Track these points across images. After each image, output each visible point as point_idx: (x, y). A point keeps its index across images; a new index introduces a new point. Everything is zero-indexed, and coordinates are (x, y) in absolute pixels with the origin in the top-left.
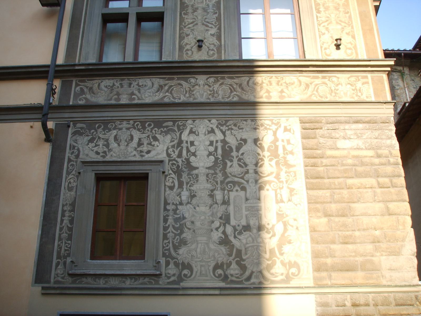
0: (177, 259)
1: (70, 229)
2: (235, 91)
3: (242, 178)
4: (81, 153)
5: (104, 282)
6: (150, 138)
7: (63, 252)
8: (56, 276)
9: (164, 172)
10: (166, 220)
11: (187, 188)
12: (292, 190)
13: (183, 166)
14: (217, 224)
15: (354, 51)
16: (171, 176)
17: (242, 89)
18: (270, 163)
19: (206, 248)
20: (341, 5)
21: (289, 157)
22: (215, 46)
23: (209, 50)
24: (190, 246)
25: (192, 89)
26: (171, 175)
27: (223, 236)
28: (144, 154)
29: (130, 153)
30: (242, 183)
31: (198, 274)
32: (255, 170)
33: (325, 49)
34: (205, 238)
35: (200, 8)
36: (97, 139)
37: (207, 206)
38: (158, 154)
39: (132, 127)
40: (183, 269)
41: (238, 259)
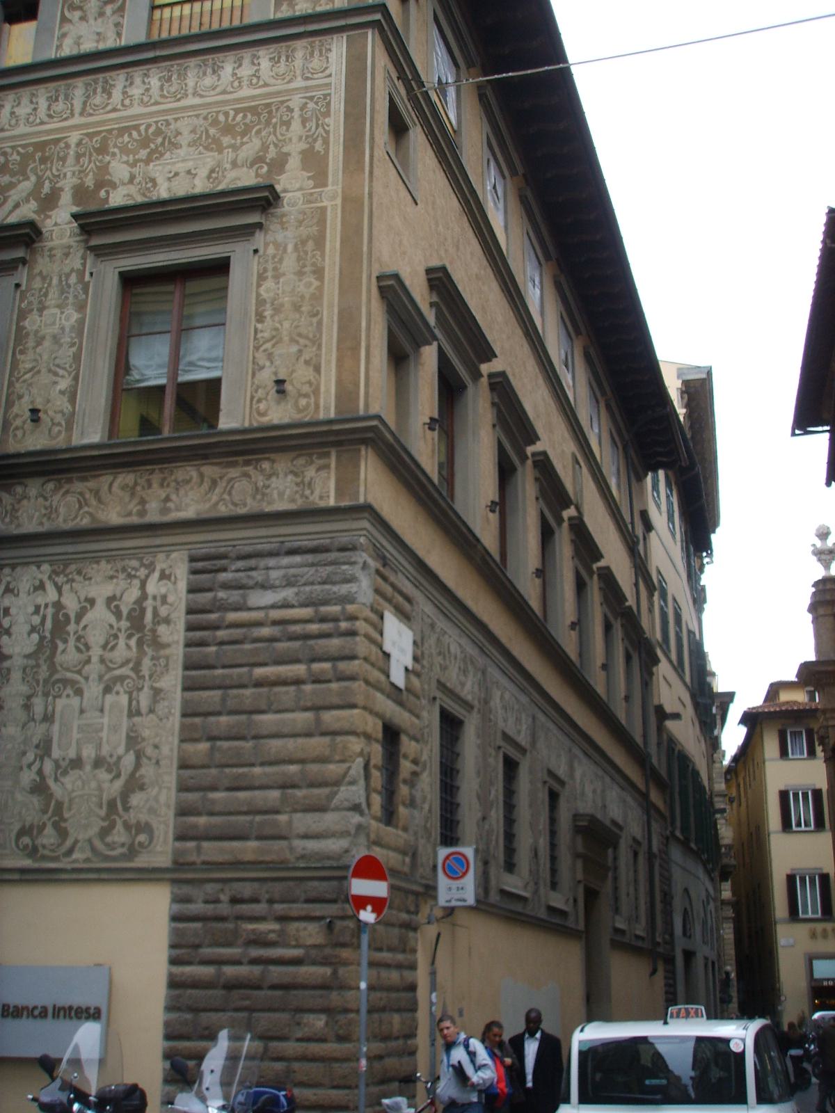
2: (86, 504)
3: (79, 672)
12: (157, 692)
14: (30, 756)
15: (313, 400)
17: (100, 501)
19: (10, 801)
20: (307, 296)
21: (162, 629)
22: (64, 414)
23: (53, 424)
25: (17, 506)
27: (38, 779)
32: (101, 656)
33: (259, 401)
35: (47, 337)
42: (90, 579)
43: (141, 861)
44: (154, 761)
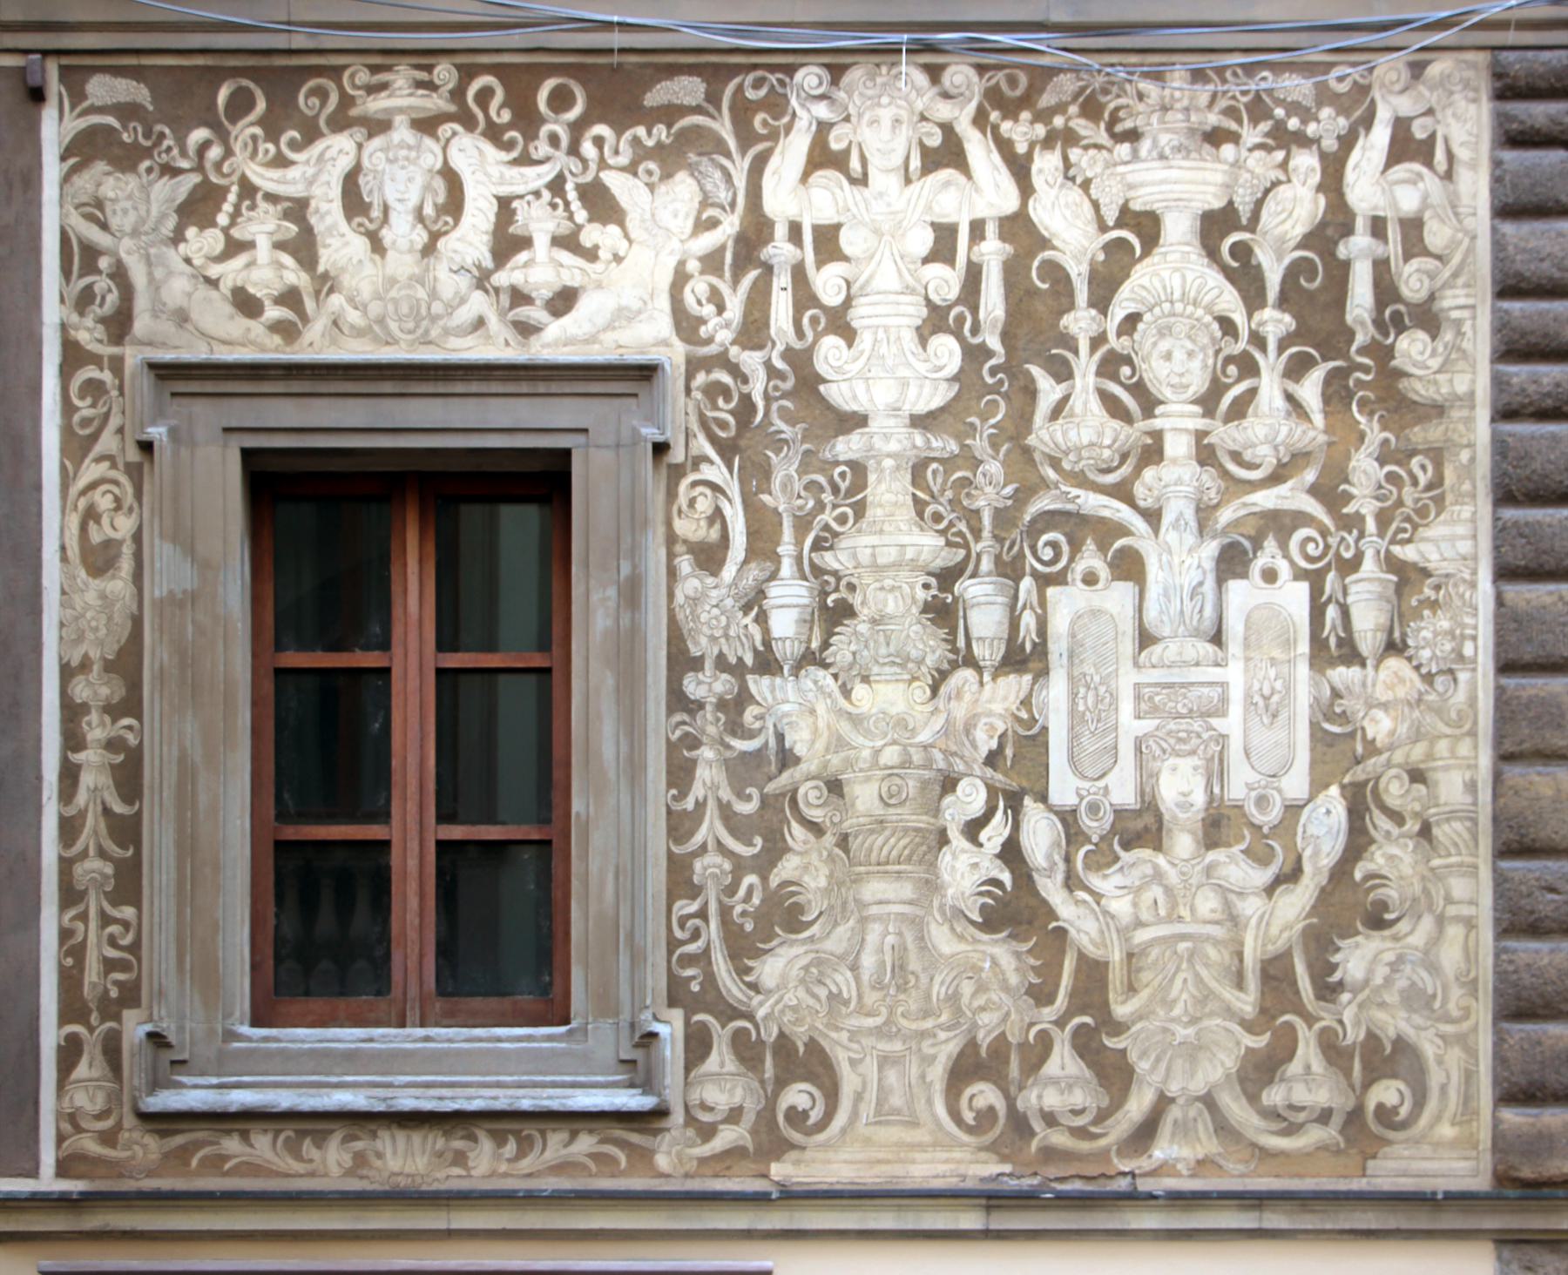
0: (750, 1017)
1: (127, 831)
3: (1122, 492)
4: (141, 303)
5: (347, 1159)
6: (572, 195)
7: (95, 979)
8: (67, 1127)
9: (660, 449)
10: (680, 773)
11: (799, 559)
12: (1406, 576)
13: (775, 406)
14: (971, 797)
16: (709, 473)
18: (1292, 387)
21: (1412, 347)
24: (821, 939)
26: (704, 467)
27: (1006, 877)
28: (535, 313)
29: (451, 309)
30: (1123, 530)
31: (867, 1110)
32: (1200, 435)
34: (907, 890)
36: (232, 197)
37: (915, 679)
38: (624, 316)
39: (452, 108)
40: (781, 1083)
41: (1087, 1019)
42: (1133, 136)
43: (1395, 1168)
44: (1412, 826)
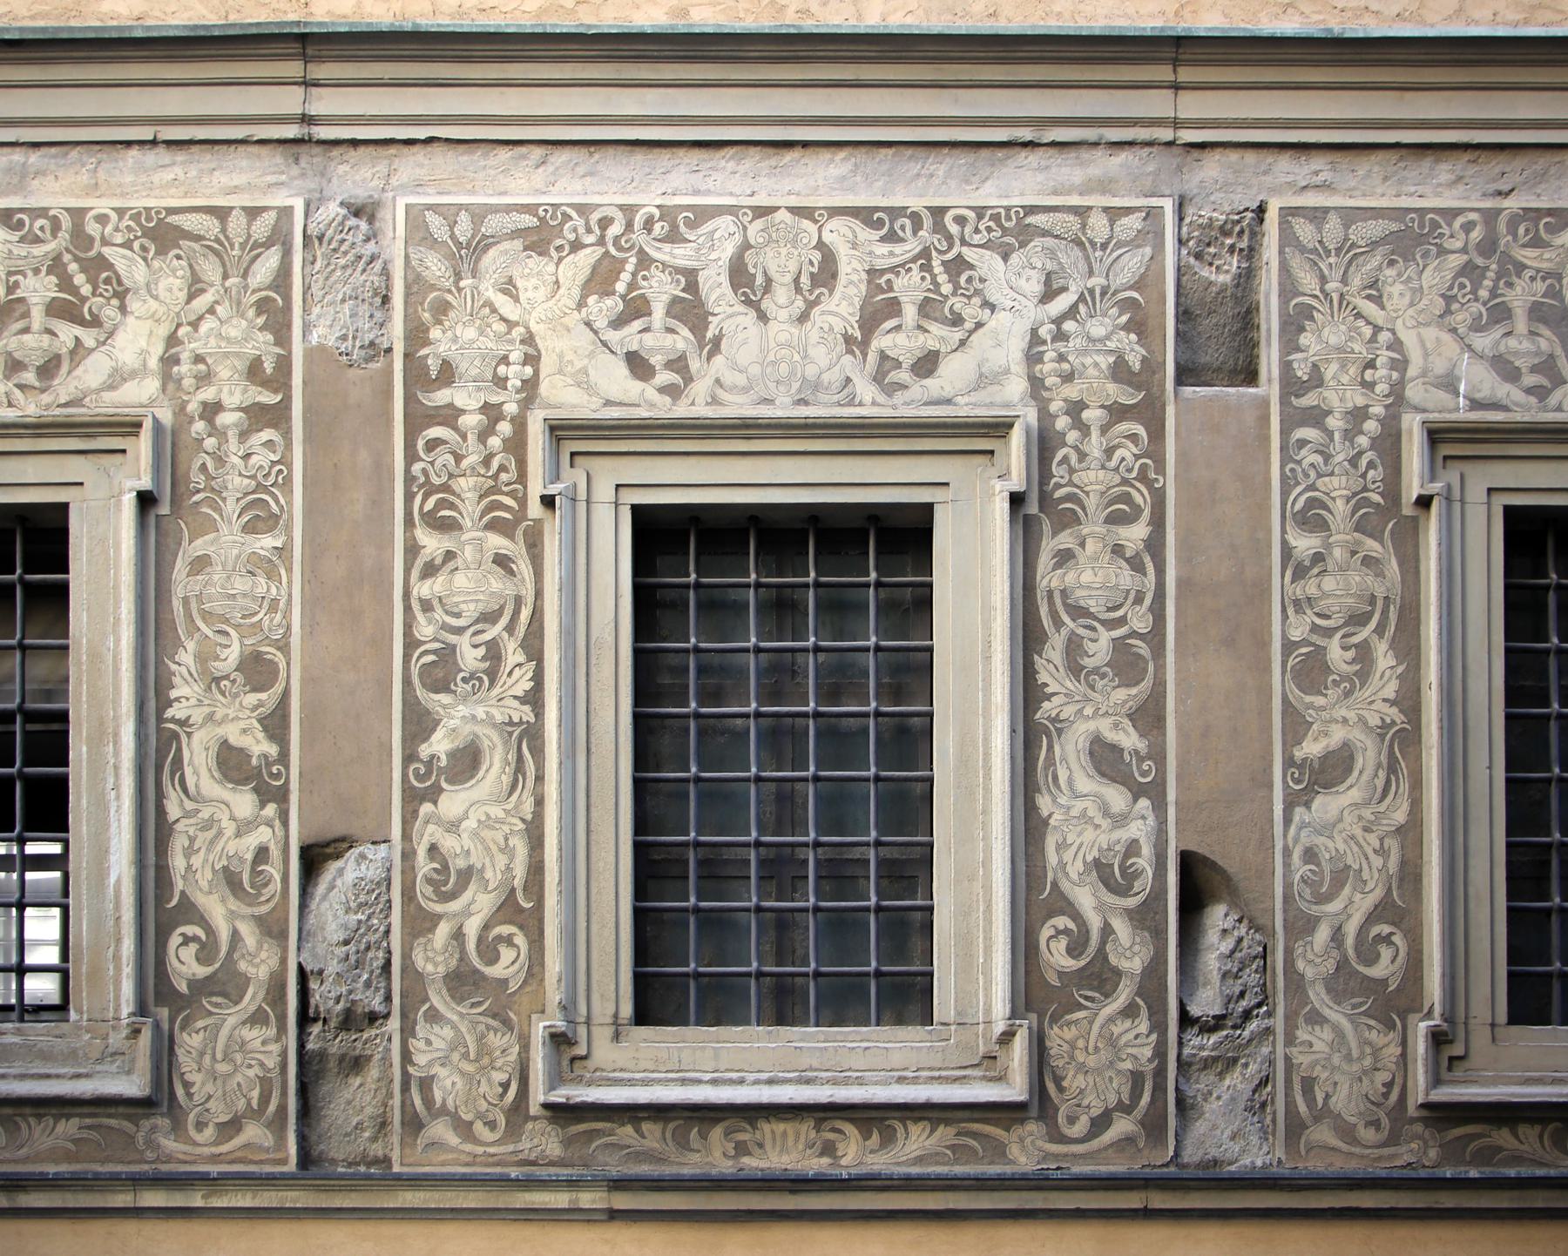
28: (903, 376)
